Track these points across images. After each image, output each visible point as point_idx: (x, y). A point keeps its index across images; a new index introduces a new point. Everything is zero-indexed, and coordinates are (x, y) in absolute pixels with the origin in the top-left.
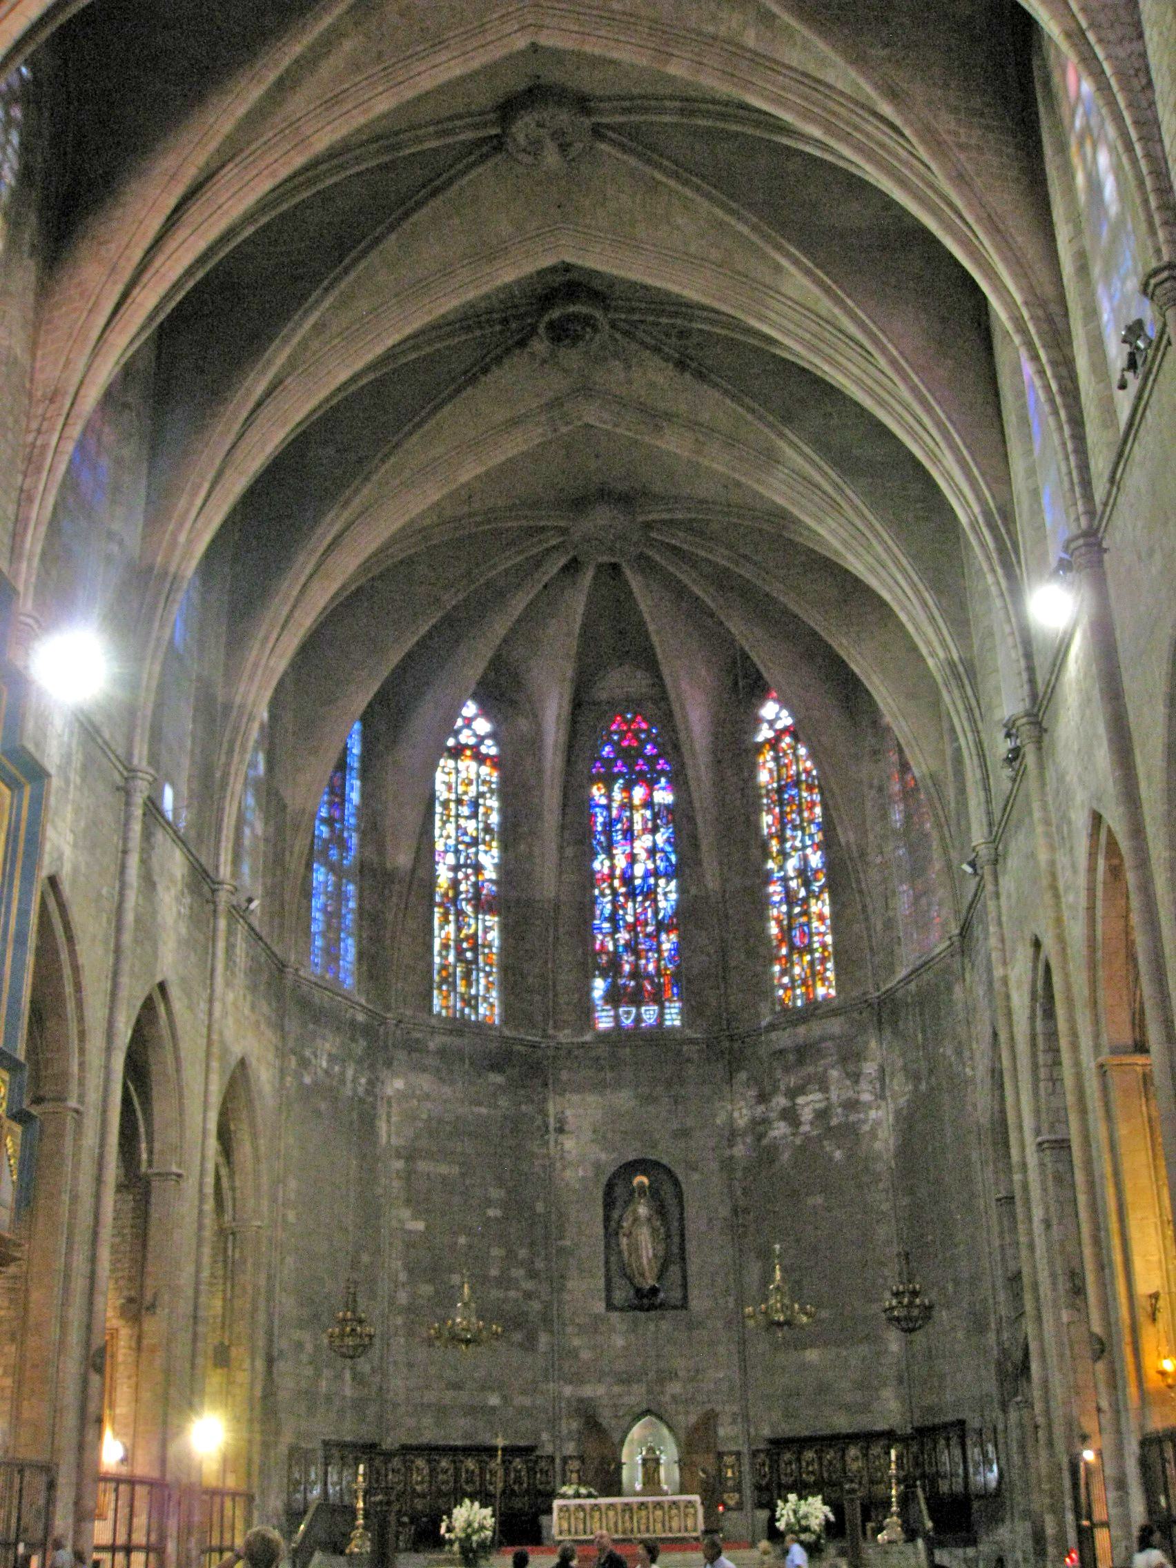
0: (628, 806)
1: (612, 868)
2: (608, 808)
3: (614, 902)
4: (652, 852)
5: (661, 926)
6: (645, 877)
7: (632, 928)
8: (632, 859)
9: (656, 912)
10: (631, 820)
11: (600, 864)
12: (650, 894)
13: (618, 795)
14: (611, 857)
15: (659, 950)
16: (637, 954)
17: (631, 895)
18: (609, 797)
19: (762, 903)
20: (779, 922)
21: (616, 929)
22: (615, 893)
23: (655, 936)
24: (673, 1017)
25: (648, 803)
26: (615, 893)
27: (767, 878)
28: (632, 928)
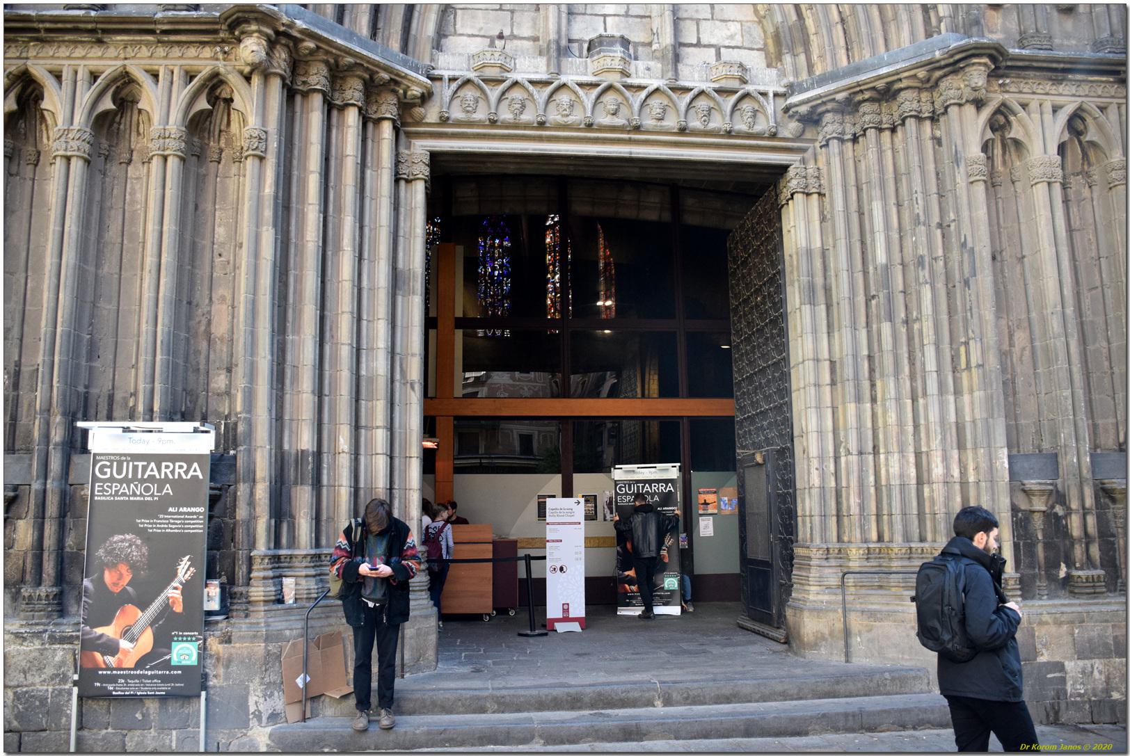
0: (493, 246)
1: (486, 272)
2: (485, 247)
3: (486, 286)
4: (501, 266)
5: (504, 297)
6: (498, 276)
7: (492, 297)
8: (494, 269)
9: (503, 290)
10: (494, 252)
11: (481, 270)
12: (500, 283)
13: (488, 242)
14: (485, 268)
15: (503, 306)
16: (494, 308)
17: (493, 283)
18: (485, 243)
19: (546, 291)
20: (551, 299)
21: (486, 297)
22: (486, 282)
23: (502, 301)
24: (507, 333)
25: (501, 246)
26: (486, 282)
27: (547, 281)
28: (492, 297)
